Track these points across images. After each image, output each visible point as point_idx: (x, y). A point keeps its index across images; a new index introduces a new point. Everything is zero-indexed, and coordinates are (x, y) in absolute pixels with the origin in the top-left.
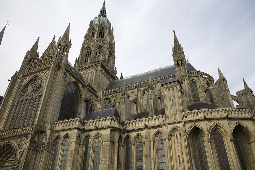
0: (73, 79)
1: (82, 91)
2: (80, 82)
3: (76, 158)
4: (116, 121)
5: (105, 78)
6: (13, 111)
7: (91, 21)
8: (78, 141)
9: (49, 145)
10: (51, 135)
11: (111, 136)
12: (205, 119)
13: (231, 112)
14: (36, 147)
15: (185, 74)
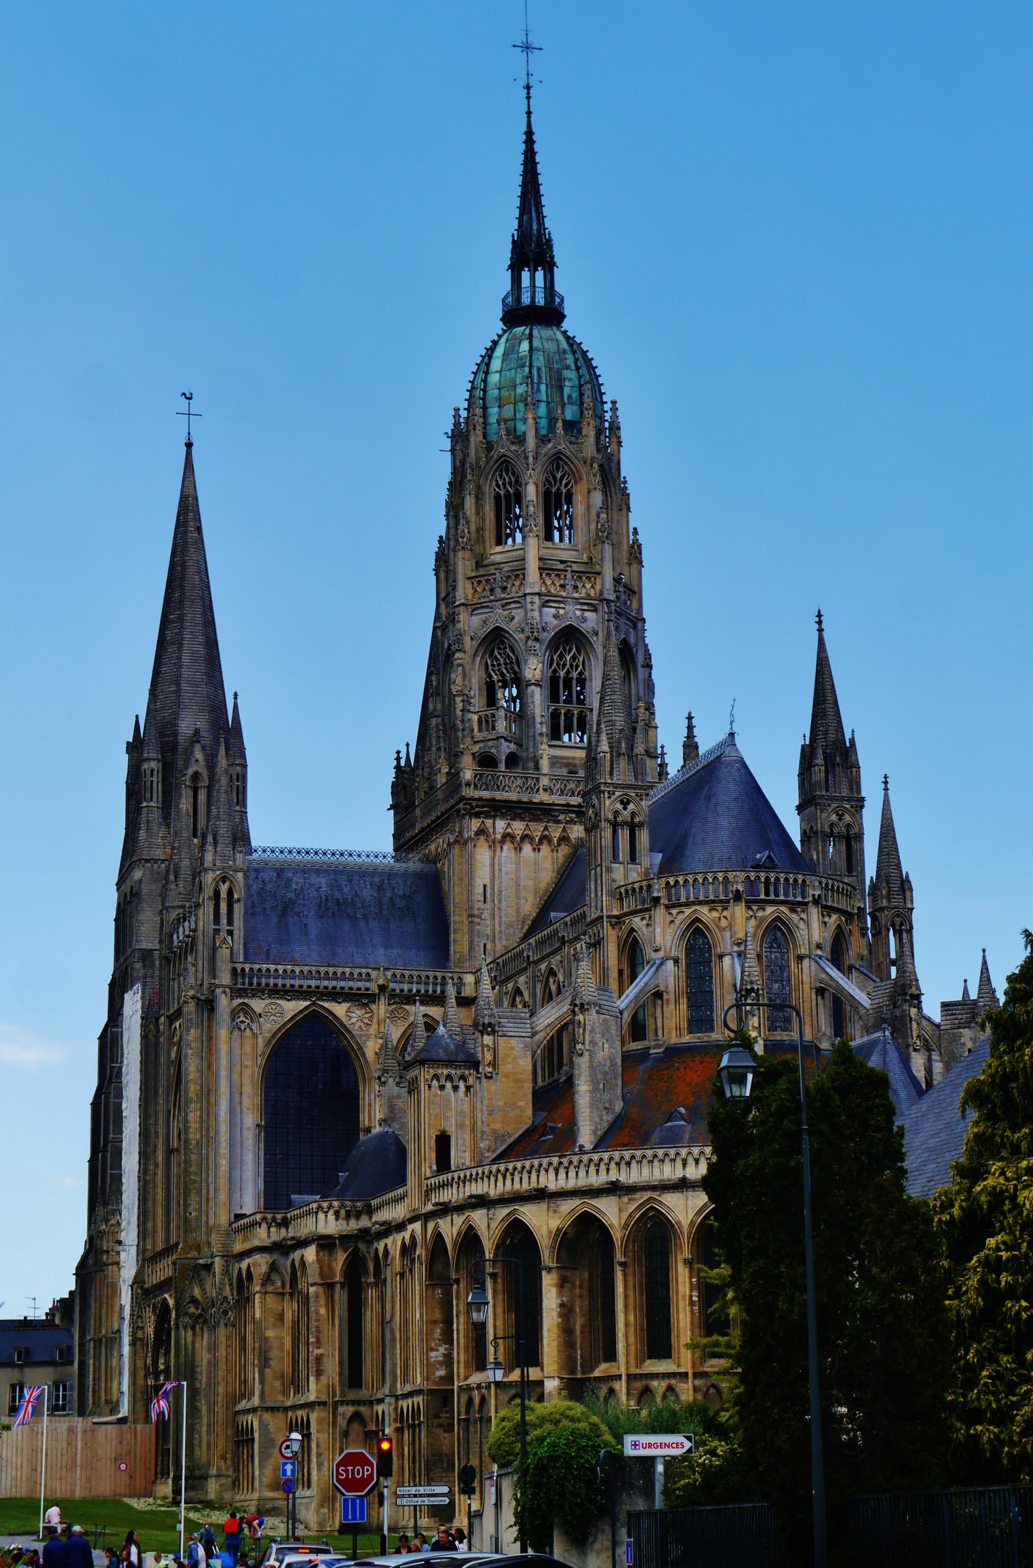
0: (292, 1007)
1: (355, 1030)
2: (336, 995)
3: (275, 1338)
4: (331, 1212)
5: (527, 848)
6: (174, 1169)
7: (457, 410)
8: (273, 1285)
9: (225, 1305)
10: (226, 1272)
11: (321, 1268)
12: (445, 1210)
13: (504, 1178)
14: (200, 1316)
15: (599, 913)
